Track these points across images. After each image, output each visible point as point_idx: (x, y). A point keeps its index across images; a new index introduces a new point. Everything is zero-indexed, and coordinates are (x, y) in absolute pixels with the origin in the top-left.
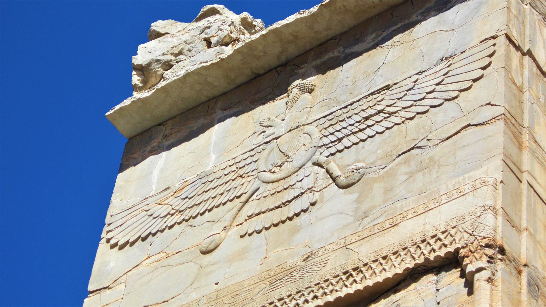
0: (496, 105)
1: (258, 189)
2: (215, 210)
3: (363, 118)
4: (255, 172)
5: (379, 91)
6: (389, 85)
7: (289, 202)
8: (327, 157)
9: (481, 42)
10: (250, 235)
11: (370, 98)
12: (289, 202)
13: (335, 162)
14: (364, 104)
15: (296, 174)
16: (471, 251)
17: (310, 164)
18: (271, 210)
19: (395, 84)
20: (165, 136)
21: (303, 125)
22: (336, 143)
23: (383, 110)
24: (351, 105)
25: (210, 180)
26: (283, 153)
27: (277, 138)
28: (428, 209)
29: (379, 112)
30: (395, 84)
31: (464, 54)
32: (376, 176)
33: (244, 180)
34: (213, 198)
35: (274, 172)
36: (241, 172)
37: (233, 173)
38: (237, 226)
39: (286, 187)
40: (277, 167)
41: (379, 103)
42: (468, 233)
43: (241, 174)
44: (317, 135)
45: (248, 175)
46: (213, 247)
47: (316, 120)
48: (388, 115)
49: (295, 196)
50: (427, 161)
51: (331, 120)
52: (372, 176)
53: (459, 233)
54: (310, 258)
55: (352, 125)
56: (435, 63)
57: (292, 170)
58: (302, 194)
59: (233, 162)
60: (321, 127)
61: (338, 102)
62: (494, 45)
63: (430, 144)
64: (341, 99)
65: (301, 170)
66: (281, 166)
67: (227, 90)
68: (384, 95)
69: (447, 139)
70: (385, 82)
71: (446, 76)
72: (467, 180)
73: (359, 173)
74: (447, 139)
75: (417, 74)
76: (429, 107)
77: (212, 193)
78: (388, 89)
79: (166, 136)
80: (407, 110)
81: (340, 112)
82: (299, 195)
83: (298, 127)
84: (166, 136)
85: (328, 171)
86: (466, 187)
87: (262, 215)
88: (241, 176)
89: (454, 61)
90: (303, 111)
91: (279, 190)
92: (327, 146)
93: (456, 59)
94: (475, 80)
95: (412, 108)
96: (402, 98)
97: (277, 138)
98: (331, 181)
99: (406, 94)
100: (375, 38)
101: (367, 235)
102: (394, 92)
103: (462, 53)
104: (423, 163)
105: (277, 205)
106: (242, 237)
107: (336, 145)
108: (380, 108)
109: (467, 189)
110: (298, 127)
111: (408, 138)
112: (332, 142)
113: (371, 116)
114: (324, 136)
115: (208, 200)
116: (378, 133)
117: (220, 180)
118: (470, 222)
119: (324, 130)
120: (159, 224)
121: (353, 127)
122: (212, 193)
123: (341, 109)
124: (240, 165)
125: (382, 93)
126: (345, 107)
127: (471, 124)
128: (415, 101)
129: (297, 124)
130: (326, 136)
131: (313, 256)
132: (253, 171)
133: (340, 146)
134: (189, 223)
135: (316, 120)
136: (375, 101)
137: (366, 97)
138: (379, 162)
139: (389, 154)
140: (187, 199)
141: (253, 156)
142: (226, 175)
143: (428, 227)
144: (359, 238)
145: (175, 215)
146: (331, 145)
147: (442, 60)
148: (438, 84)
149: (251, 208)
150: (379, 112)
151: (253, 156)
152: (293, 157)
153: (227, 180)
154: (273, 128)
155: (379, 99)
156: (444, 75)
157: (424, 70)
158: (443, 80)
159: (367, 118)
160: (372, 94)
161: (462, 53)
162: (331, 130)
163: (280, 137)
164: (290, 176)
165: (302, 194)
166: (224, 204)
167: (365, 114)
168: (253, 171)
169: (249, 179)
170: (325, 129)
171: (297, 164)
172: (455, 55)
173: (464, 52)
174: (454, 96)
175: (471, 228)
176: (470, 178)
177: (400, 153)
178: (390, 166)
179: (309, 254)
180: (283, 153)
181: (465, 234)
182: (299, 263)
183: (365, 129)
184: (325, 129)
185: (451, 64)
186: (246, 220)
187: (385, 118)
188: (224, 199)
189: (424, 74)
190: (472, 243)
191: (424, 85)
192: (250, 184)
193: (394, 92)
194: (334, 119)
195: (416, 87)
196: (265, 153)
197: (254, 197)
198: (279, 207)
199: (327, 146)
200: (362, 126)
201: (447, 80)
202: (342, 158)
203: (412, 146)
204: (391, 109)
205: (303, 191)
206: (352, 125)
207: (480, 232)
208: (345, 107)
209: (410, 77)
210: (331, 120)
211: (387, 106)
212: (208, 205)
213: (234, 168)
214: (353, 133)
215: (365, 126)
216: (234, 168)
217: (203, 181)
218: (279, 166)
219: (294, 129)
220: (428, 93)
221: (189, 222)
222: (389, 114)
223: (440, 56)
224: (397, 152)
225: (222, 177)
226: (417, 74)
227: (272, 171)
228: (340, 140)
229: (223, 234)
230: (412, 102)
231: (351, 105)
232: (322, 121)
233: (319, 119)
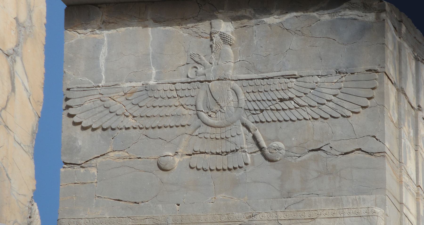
6: (295, 75)
7: (227, 153)
10: (198, 170)
12: (227, 153)
13: (260, 131)
29: (291, 99)
38: (187, 155)
41: (290, 90)
48: (298, 106)
49: (232, 150)
52: (290, 160)
54: (251, 219)
55: (270, 101)
61: (257, 71)
63: (333, 152)
69: (346, 154)
72: (362, 200)
74: (346, 154)
80: (312, 108)
82: (233, 151)
85: (254, 137)
98: (258, 149)
101: (293, 218)
104: (328, 167)
105: (218, 152)
112: (255, 110)
114: (248, 100)
116: (291, 120)
128: (318, 103)
130: (250, 101)
131: (253, 218)
137: (279, 77)
144: (287, 218)
146: (255, 113)
150: (291, 99)
152: (225, 109)
159: (282, 100)
176: (364, 200)
177: (311, 149)
178: (304, 157)
179: (251, 215)
182: (243, 219)
186: (194, 154)
187: (295, 107)
193: (301, 84)
198: (218, 154)
206: (270, 101)
211: (297, 96)
214: (272, 110)
228: (262, 111)
231: (268, 79)
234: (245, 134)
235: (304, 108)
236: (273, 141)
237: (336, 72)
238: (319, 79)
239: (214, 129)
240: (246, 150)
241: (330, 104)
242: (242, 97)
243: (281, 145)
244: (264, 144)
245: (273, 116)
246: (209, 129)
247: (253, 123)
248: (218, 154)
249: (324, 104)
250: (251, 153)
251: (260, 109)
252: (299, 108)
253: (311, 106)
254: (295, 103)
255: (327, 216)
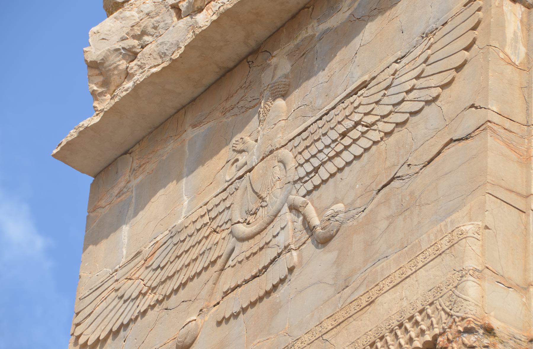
0: (481, 108)
1: (233, 250)
2: (190, 284)
3: (340, 134)
4: (228, 225)
5: (355, 92)
6: (366, 81)
7: (266, 268)
8: (304, 196)
9: (465, 6)
11: (347, 102)
12: (266, 268)
14: (340, 113)
15: (271, 226)
16: (448, 339)
17: (286, 208)
18: (247, 282)
19: (374, 78)
20: (133, 171)
21: (277, 149)
22: (313, 174)
23: (361, 120)
24: (326, 114)
25: (182, 239)
26: (256, 193)
27: (250, 171)
28: (404, 276)
29: (357, 124)
30: (374, 78)
31: (446, 26)
32: (355, 223)
33: (219, 236)
34: (186, 266)
35: (248, 224)
36: (214, 225)
37: (206, 227)
38: (214, 306)
39: (261, 246)
40: (251, 215)
42: (446, 313)
43: (215, 227)
44: (292, 164)
45: (222, 228)
46: (190, 342)
47: (290, 141)
48: (366, 129)
50: (407, 199)
51: (306, 139)
53: (437, 312)
56: (414, 42)
57: (267, 220)
58: (279, 255)
59: (205, 209)
60: (296, 151)
62: (479, 10)
64: (316, 105)
65: (277, 219)
66: (255, 213)
67: (195, 95)
68: (361, 97)
70: (362, 75)
71: (427, 63)
73: (337, 221)
75: (396, 62)
76: (408, 115)
77: (185, 259)
78: (366, 87)
79: (134, 170)
80: (385, 120)
81: (315, 126)
82: (275, 258)
83: (271, 152)
84: (134, 170)
86: (443, 241)
87: (239, 290)
88: (215, 231)
89: (436, 37)
90: (276, 127)
91: (254, 251)
92: (303, 181)
93: (439, 34)
94: (458, 69)
95: (391, 116)
96: (380, 100)
97: (250, 171)
99: (384, 95)
100: (350, 4)
102: (372, 91)
103: (443, 25)
106: (219, 323)
107: (312, 181)
108: (356, 117)
109: (444, 244)
110: (271, 152)
111: (388, 164)
112: (308, 174)
113: (349, 130)
115: (181, 269)
117: (193, 237)
118: (448, 294)
119: (299, 156)
120: (131, 311)
121: (330, 149)
122: (185, 259)
123: (315, 122)
124: (213, 214)
125: (360, 93)
126: (320, 119)
127: (454, 139)
128: (394, 105)
129: (270, 148)
132: (227, 223)
133: (317, 180)
134: (165, 304)
135: (290, 141)
136: (351, 108)
137: (342, 101)
138: (358, 203)
139: (368, 190)
140: (159, 270)
141: (226, 199)
142: (198, 230)
143: (405, 303)
145: (148, 294)
146: (307, 178)
147: (423, 37)
148: (418, 78)
149: (228, 280)
150: (357, 124)
151: (226, 199)
152: (267, 199)
153: (200, 239)
154: (246, 153)
155: (356, 104)
156: (425, 62)
157: (403, 55)
158: (422, 72)
159: (344, 135)
160: (349, 96)
161: (443, 25)
162: (306, 155)
163: (253, 168)
164: (265, 228)
165: (279, 255)
166: (199, 274)
167: (341, 129)
168: (227, 223)
169: (224, 234)
170: (300, 153)
171: (271, 210)
172: (437, 29)
173: (446, 23)
174: (435, 95)
175: (448, 304)
180: (256, 193)
181: (442, 312)
183: (341, 152)
184: (300, 153)
185: (432, 44)
186: (223, 298)
188: (198, 267)
189: (404, 61)
190: (450, 328)
191: (403, 79)
192: (226, 242)
193: (372, 91)
194: (309, 138)
195: (396, 82)
196: (239, 193)
197: (230, 263)
198: (254, 277)
199: (303, 181)
200: (340, 148)
201: (429, 70)
202: (319, 197)
203: (392, 176)
204: (369, 119)
205: (280, 251)
207: (458, 310)
208: (320, 119)
209: (388, 67)
210: (306, 139)
212: (182, 278)
213: (206, 219)
215: (342, 147)
216: (206, 219)
217: (175, 240)
218: (253, 214)
219: (267, 156)
220: (408, 92)
221: (164, 303)
222: (367, 126)
223: (421, 30)
224: (377, 185)
225: (195, 234)
226: (396, 62)
227: (247, 221)
228: (316, 170)
229: (200, 321)
230: (390, 108)
231: (326, 114)
232: (298, 140)
233: (293, 139)
234: (294, 222)
235: (375, 127)
236: (328, 208)
237: (423, 37)
238: (397, 66)
239: (252, 241)
240: (292, 246)
241: (411, 96)
242: (292, 164)
243: (340, 207)
244: (315, 221)
245: (331, 167)
246: (246, 245)
247: (304, 196)
248: (254, 277)
249: (403, 101)
250: (299, 247)
251: (315, 168)
252: (367, 131)
253: (383, 117)
254: (363, 125)
255: (391, 285)
